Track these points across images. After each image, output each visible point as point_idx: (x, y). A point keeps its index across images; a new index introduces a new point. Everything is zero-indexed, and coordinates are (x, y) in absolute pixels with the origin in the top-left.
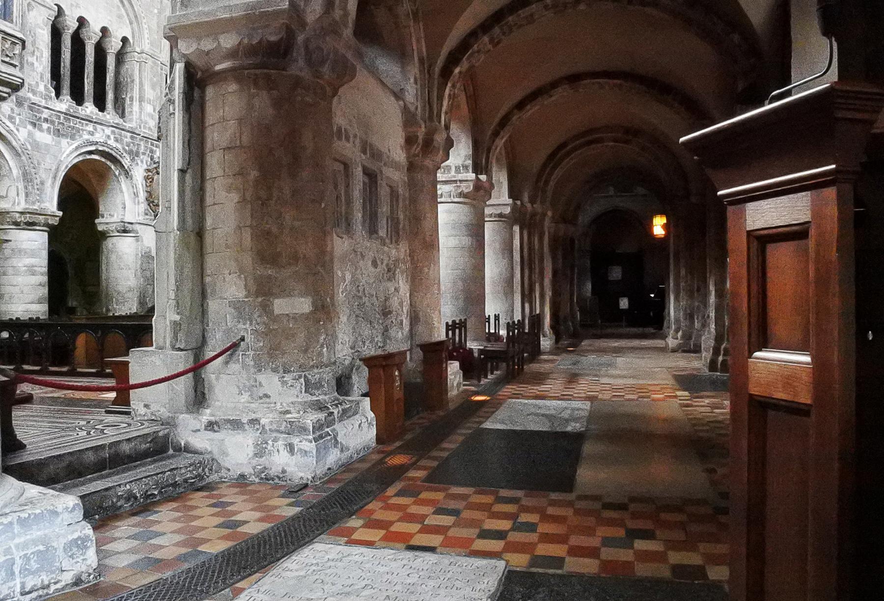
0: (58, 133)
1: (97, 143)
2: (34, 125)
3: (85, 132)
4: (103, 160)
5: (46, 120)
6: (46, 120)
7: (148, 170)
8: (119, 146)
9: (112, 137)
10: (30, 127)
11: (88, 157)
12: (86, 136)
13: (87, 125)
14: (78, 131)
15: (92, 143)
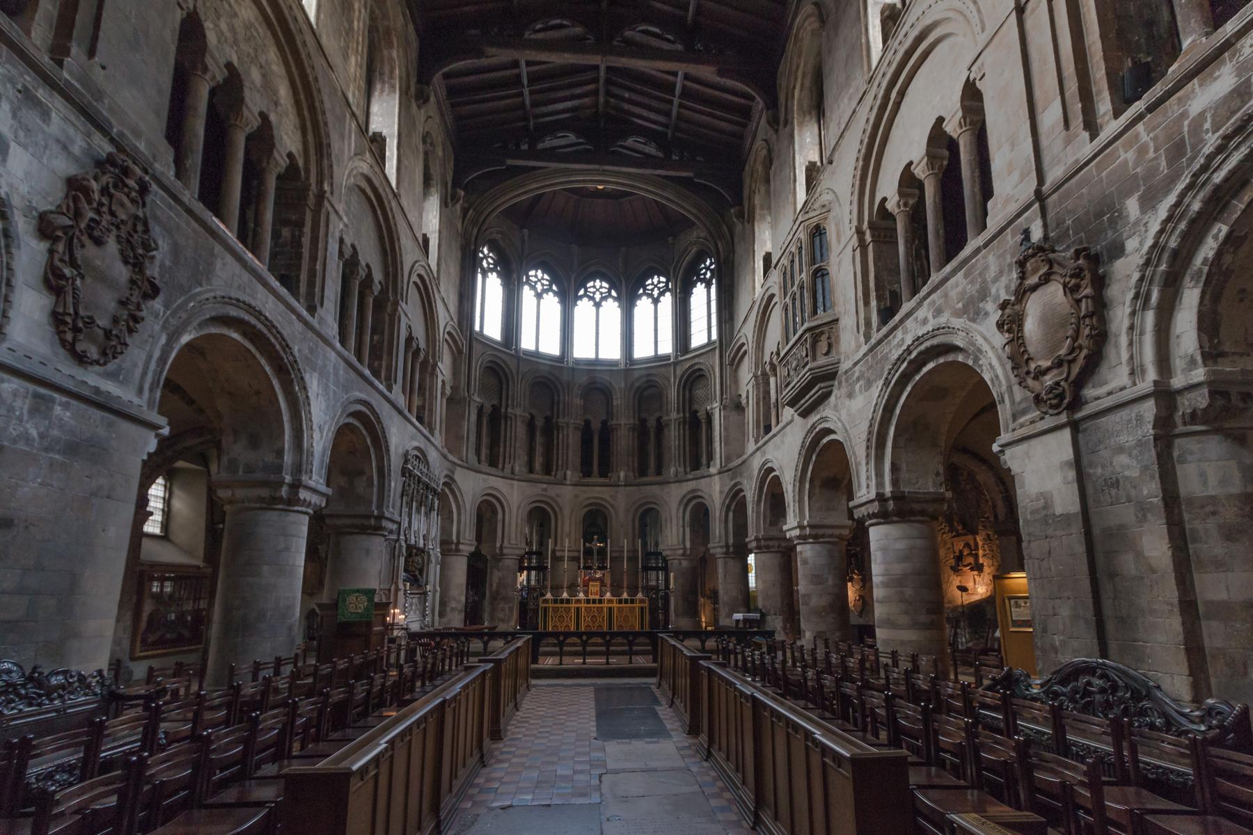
0: (869, 384)
1: (909, 351)
2: (850, 395)
3: (893, 351)
4: (941, 360)
5: (858, 379)
6: (858, 379)
7: (1004, 306)
8: (942, 320)
9: (930, 317)
10: (847, 402)
11: (917, 378)
12: (895, 355)
13: (894, 337)
14: (886, 358)
15: (901, 359)
